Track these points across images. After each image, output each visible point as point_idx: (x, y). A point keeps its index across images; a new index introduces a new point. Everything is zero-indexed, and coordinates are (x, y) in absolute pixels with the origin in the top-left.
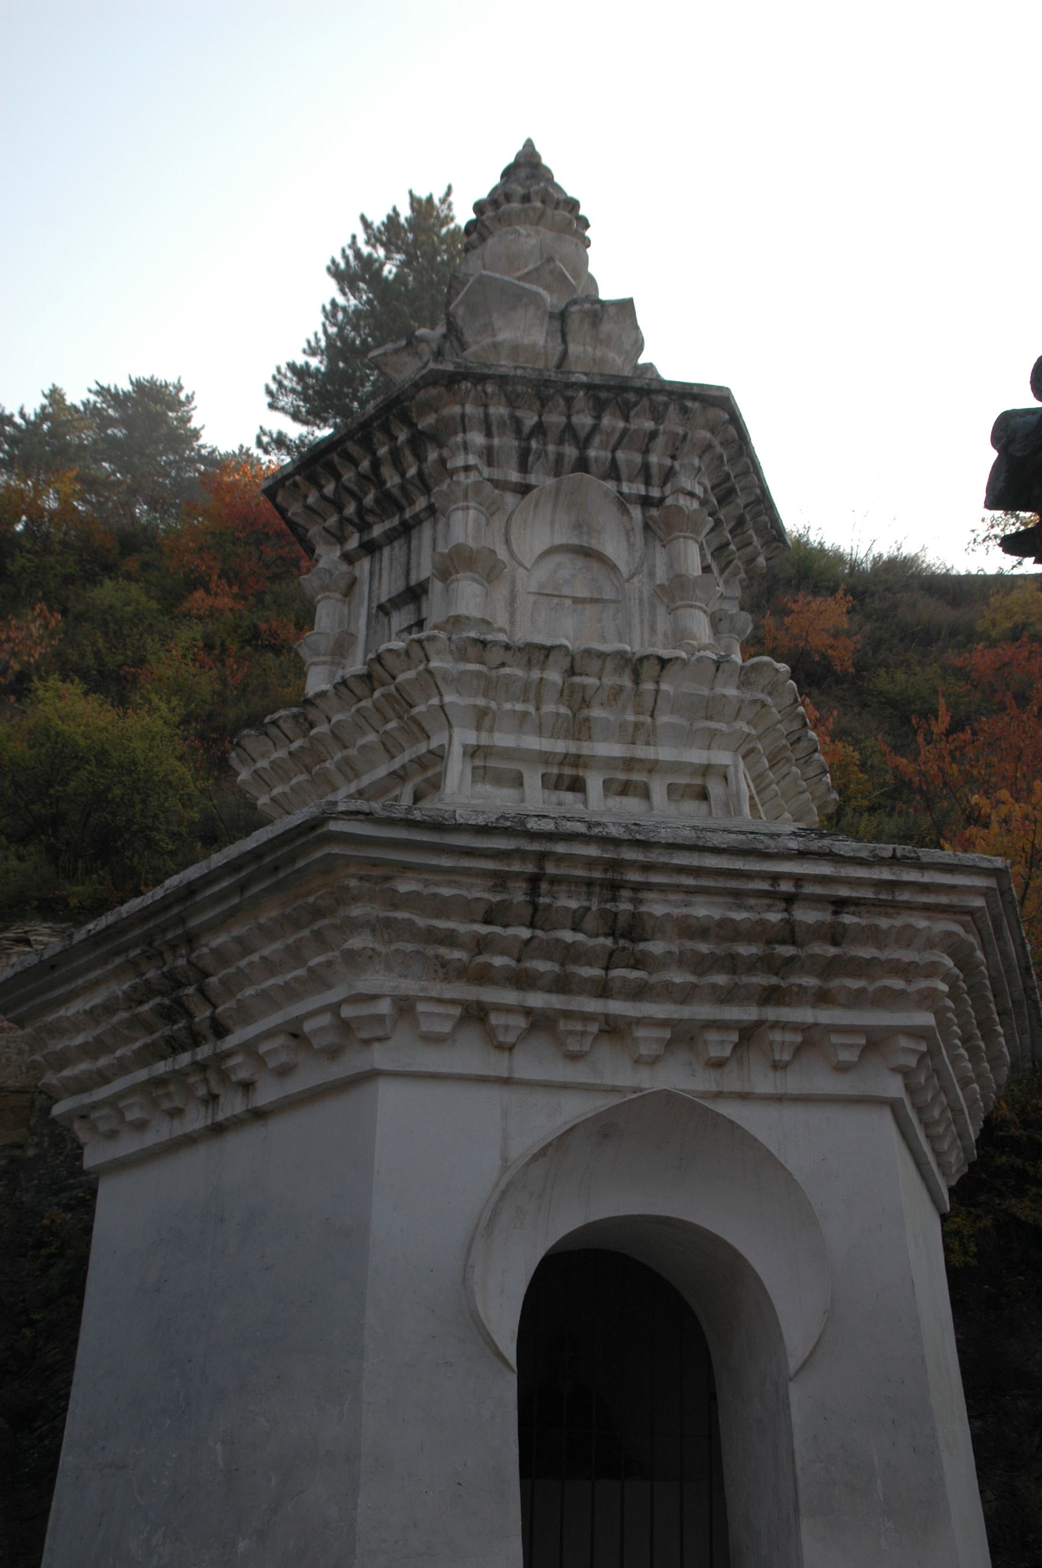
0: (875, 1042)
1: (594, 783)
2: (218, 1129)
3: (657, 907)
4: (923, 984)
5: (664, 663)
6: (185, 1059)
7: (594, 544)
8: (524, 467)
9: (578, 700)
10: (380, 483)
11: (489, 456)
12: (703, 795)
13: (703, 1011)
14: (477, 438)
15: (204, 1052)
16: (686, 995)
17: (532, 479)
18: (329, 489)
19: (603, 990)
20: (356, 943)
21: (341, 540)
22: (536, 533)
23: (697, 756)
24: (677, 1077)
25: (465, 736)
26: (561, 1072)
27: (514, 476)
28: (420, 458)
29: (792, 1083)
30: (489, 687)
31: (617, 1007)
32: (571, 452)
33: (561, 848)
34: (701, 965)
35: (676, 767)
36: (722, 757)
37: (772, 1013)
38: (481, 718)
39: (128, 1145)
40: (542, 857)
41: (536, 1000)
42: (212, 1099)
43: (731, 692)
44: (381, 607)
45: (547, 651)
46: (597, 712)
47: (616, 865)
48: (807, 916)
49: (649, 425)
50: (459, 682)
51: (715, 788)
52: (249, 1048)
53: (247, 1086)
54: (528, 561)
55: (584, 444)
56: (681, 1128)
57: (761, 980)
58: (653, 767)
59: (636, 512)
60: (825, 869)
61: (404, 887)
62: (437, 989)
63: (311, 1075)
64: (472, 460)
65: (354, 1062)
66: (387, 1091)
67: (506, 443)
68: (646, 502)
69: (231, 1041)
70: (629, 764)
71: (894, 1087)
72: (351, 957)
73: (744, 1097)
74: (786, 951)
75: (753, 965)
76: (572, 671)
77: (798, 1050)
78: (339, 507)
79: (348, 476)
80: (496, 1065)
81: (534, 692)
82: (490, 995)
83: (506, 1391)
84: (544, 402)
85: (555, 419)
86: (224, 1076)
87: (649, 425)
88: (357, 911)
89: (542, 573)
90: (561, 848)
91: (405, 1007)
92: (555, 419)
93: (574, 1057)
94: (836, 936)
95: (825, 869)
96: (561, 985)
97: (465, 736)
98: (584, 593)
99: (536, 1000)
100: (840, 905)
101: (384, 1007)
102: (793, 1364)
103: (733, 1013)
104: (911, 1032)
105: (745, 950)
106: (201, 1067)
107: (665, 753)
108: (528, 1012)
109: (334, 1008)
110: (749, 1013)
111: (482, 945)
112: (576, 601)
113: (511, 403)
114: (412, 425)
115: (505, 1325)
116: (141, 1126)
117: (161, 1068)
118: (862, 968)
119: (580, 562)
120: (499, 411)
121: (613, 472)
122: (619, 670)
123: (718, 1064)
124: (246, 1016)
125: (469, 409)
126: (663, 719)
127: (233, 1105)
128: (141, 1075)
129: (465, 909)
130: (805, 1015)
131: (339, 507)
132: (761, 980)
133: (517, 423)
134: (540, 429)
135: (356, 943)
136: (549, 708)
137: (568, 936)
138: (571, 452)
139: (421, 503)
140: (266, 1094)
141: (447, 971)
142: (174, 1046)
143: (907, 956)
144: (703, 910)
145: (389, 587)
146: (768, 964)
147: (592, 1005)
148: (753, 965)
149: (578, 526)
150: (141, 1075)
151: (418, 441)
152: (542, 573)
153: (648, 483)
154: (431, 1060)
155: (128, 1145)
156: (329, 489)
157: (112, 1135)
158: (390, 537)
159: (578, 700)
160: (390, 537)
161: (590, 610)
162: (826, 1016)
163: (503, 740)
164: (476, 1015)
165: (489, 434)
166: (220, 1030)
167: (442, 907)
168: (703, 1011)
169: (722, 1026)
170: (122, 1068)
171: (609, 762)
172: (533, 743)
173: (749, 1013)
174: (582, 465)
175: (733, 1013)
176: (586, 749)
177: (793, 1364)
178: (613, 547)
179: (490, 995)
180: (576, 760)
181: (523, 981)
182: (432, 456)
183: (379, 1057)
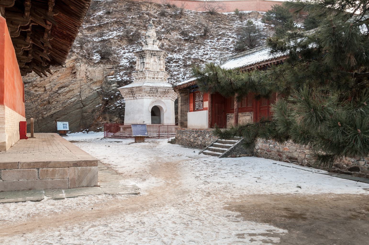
1: (155, 78)
3: (159, 90)
11: (149, 55)
22: (152, 60)
23: (161, 77)
24: (159, 98)
30: (149, 73)
36: (163, 77)
38: (148, 75)
48: (166, 90)
63: (140, 98)
65: (142, 97)
66: (144, 99)
67: (150, 54)
71: (171, 98)
80: (150, 98)
83: (150, 114)
85: (153, 53)
91: (145, 95)
92: (153, 53)
115: (150, 111)
121: (157, 56)
144: (161, 90)
145: (142, 62)
154: (147, 97)
163: (150, 76)
172: (152, 76)
174: (155, 56)
178: (157, 61)
183: (144, 97)
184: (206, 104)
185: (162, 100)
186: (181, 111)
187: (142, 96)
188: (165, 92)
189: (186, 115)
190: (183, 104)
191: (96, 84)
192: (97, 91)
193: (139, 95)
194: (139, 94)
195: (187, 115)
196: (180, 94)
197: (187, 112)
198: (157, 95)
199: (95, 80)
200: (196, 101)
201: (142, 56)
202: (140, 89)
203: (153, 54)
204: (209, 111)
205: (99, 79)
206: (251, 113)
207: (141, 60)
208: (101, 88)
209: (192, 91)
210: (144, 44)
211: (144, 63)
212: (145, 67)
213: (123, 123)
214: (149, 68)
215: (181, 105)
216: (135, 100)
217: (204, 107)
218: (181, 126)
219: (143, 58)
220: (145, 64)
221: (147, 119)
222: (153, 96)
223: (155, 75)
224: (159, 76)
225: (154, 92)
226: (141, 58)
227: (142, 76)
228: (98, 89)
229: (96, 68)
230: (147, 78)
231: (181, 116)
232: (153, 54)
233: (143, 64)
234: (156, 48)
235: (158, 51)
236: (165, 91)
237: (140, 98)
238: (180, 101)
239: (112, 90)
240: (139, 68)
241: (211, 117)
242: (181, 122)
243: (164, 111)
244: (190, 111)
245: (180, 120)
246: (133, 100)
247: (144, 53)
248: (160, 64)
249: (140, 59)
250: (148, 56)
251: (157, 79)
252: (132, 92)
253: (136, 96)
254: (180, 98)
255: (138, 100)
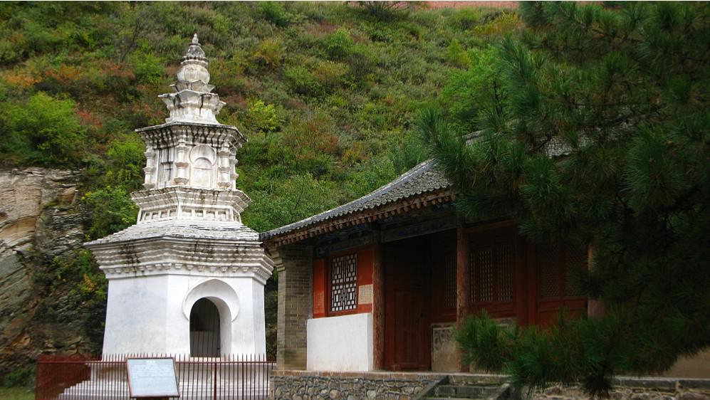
0: (250, 268)
1: (205, 212)
2: (136, 277)
4: (259, 259)
5: (219, 192)
6: (131, 265)
7: (207, 157)
8: (193, 141)
9: (203, 198)
10: (163, 139)
11: (187, 139)
12: (225, 213)
13: (222, 264)
14: (185, 136)
15: (135, 265)
16: (219, 262)
17: (195, 143)
18: (151, 136)
19: (206, 261)
20: (166, 254)
21: (153, 146)
22: (196, 155)
23: (224, 207)
24: (217, 274)
25: (181, 204)
26: (198, 274)
27: (191, 143)
28: (172, 137)
29: (236, 275)
30: (186, 196)
31: (208, 264)
32: (203, 138)
33: (201, 240)
34: (222, 257)
35: (220, 209)
36: (229, 207)
37: (234, 264)
38: (184, 201)
39: (116, 276)
40: (197, 242)
41: (195, 263)
42: (136, 272)
43: (231, 196)
44: (162, 163)
45: (198, 190)
46: (206, 200)
47: (210, 243)
48: (240, 249)
49: (219, 134)
50: (181, 195)
51: (227, 213)
52: (145, 266)
53: (143, 271)
54: (193, 161)
55: (206, 137)
56: (217, 284)
57: (232, 259)
58: (215, 209)
59: (215, 150)
60: (244, 242)
61: (175, 246)
62: (178, 261)
63: (155, 272)
64: (183, 141)
66: (169, 276)
67: (190, 137)
68: (217, 148)
69: (141, 264)
70: (211, 208)
71: (253, 275)
72: (165, 256)
73: (228, 277)
74: (236, 255)
75: (231, 257)
76: (202, 193)
77: (237, 270)
78: (153, 140)
79: (156, 136)
80: (188, 273)
81: (195, 197)
82: (187, 262)
84: (198, 130)
85: (200, 133)
86: (138, 269)
87: (219, 134)
88: (166, 249)
89: (196, 164)
90: (201, 240)
91: (173, 264)
92: (200, 133)
93: (200, 271)
94: (245, 252)
95: (244, 242)
96: (199, 260)
97: (181, 204)
98: (204, 168)
99: (195, 263)
100: (246, 247)
101: (170, 265)
102: (233, 319)
103: (228, 264)
104: (257, 267)
105: (230, 255)
106: (134, 267)
107: (218, 206)
108: (193, 265)
109: (161, 264)
110: (230, 264)
111: (186, 255)
112: (203, 169)
113: (192, 130)
114: (171, 131)
116: (120, 273)
117: (125, 265)
118: (248, 257)
119: (204, 161)
120: (189, 131)
121: (212, 142)
122: (211, 193)
123: (224, 272)
124: (144, 261)
125: (184, 131)
126: (218, 200)
127: (139, 274)
128: (121, 266)
129: (184, 250)
130: (239, 264)
131: (153, 140)
132: (232, 259)
133: (193, 134)
134: (197, 134)
135: (166, 254)
136: (197, 199)
137: (201, 253)
138: (203, 138)
139: (171, 145)
140: (146, 274)
141: (180, 259)
142: (129, 263)
143: (256, 255)
145: (164, 159)
146: (233, 257)
147: (204, 264)
148: (231, 257)
149: (204, 154)
150: (121, 266)
151: (172, 134)
152: (196, 164)
153: (218, 144)
155: (116, 276)
156: (151, 136)
157: (113, 274)
158: (164, 148)
159: (203, 198)
160: (164, 148)
161: (205, 171)
162: (242, 264)
163: (188, 204)
164: (185, 265)
165: (187, 135)
166: (138, 262)
167: (180, 249)
168: (222, 264)
169: (225, 266)
170: (116, 264)
171: (208, 208)
172: (194, 205)
173: (230, 264)
174: (205, 142)
175: (228, 264)
176: (204, 206)
177: (233, 319)
178: (210, 157)
179: (187, 262)
180: (202, 208)
181: (192, 260)
182: (175, 137)
183: (168, 272)
184: (367, 294)
185: (225, 280)
186: (287, 315)
187: (163, 268)
188: (236, 252)
189: (304, 329)
190: (292, 291)
191: (14, 229)
192: (19, 253)
193: (154, 266)
194: (153, 259)
195: (305, 328)
196: (285, 260)
197: (307, 318)
198: (208, 264)
199: (12, 216)
200: (336, 285)
201: (164, 142)
202: (157, 243)
203: (199, 133)
204: (376, 316)
205: (24, 213)
206: (507, 321)
207: (160, 155)
208: (33, 240)
209: (322, 252)
210: (172, 105)
211: (169, 163)
212: (174, 176)
213: (98, 355)
214: (186, 181)
215: (288, 297)
216: (141, 281)
217: (361, 302)
218: (287, 362)
219: (168, 148)
220: (174, 167)
221: (179, 343)
222: (196, 266)
223: (203, 202)
224: (218, 206)
225: (200, 256)
226: (160, 149)
227: (164, 206)
228: (21, 244)
229: (16, 178)
230: (180, 209)
231: (287, 332)
232: (199, 133)
233: (166, 167)
234: (207, 117)
235: (213, 128)
236: (237, 252)
237: (155, 272)
238: (284, 284)
239: (66, 247)
240: (155, 181)
241: (382, 336)
242: (286, 352)
243: (233, 316)
244: (315, 316)
245: (283, 343)
246: (132, 281)
247: (172, 134)
248: (222, 169)
249: (158, 152)
250: (182, 141)
251: (212, 215)
252: (130, 252)
253: (142, 269)
254: (284, 273)
255: (148, 279)
